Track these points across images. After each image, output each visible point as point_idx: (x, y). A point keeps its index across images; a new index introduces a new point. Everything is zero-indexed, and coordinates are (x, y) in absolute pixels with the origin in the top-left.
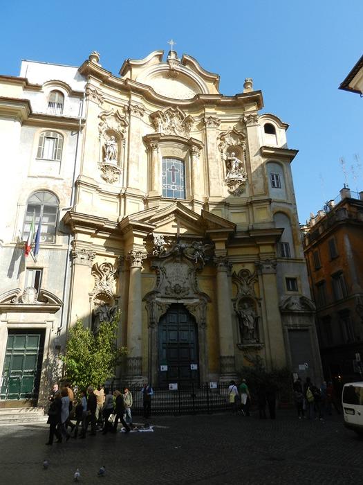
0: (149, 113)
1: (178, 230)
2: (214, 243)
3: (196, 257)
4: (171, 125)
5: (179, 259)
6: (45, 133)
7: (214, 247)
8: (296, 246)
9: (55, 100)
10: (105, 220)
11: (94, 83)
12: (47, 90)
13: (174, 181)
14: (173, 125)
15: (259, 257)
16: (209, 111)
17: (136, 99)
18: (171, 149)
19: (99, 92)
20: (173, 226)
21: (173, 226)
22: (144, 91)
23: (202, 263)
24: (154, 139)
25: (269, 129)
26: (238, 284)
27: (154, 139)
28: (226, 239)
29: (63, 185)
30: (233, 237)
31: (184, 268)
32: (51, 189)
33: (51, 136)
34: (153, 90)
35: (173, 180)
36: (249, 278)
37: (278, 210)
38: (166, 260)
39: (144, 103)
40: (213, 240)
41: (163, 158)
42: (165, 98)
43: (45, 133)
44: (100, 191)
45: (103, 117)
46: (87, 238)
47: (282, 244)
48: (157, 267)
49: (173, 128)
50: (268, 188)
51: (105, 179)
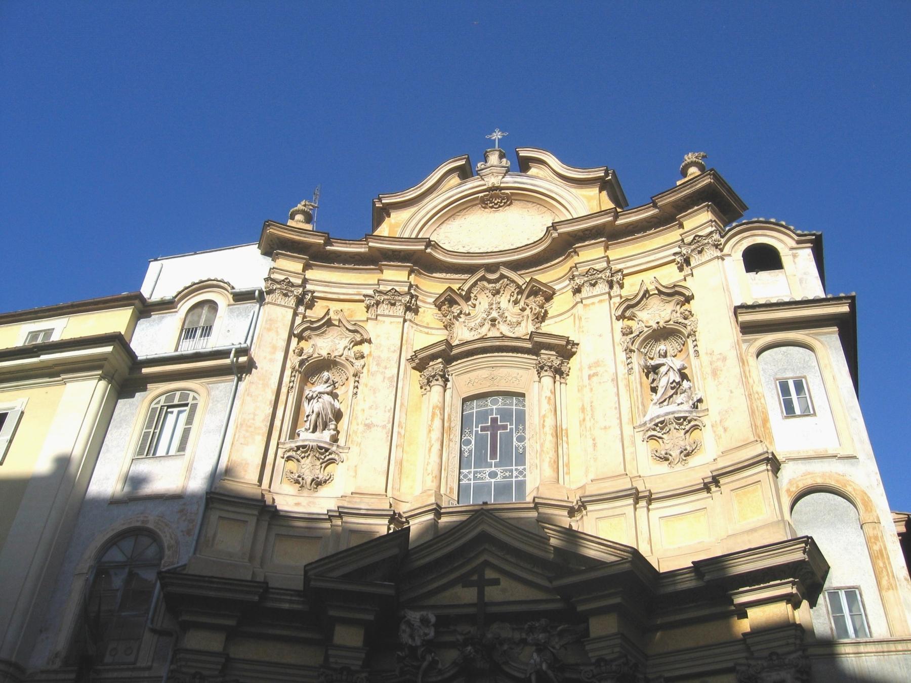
0: (432, 300)
1: (481, 594)
2: (584, 618)
6: (163, 398)
7: (587, 629)
8: (884, 593)
9: (198, 322)
10: (265, 588)
11: (291, 266)
12: (184, 307)
13: (493, 456)
14: (494, 314)
15: (748, 648)
16: (591, 254)
18: (484, 373)
22: (415, 252)
24: (434, 357)
25: (762, 259)
27: (434, 357)
28: (617, 600)
29: (182, 511)
32: (151, 526)
33: (176, 402)
34: (436, 246)
35: (493, 456)
37: (809, 482)
40: (581, 608)
41: (465, 400)
42: (469, 254)
43: (163, 398)
46: (213, 642)
47: (834, 595)
49: (493, 320)
50: (765, 421)
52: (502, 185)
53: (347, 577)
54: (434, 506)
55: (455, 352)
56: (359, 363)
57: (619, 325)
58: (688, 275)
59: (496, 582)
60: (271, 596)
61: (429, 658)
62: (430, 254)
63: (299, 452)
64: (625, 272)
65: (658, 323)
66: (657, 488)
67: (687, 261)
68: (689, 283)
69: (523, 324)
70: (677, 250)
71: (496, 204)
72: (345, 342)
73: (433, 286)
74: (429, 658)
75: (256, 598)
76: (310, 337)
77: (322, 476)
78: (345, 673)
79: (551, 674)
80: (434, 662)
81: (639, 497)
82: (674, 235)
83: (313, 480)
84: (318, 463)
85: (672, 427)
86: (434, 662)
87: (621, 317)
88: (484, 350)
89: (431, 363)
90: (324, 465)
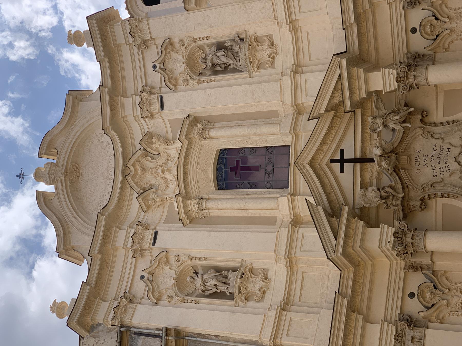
1: (349, 161)
3: (398, 127)
4: (158, 174)
5: (404, 160)
17: (122, 237)
19: (116, 303)
20: (342, 170)
21: (342, 170)
23: (410, 113)
26: (449, 40)
28: (362, 70)
30: (358, 58)
31: (422, 145)
36: (437, 19)
38: (407, 181)
39: (127, 224)
40: (364, 95)
44: (285, 306)
45: (157, 295)
48: (422, 200)
51: (264, 292)
52: (64, 167)
53: (336, 238)
54: (290, 195)
55: (183, 191)
56: (182, 258)
57: (182, 86)
58: (155, 41)
59: (342, 152)
60: (344, 291)
61: (388, 189)
62: (109, 214)
63: (243, 292)
64: (144, 84)
65: (183, 63)
66: (290, 61)
67: (145, 42)
68: (159, 42)
69: (169, 151)
70: (135, 48)
71: (77, 175)
72: (167, 269)
73: (134, 208)
74: (388, 189)
75: (346, 300)
76: (159, 292)
77: (261, 276)
78: (397, 235)
79: (400, 115)
80: (390, 187)
81: (297, 69)
82: (125, 50)
83: (263, 281)
84: (251, 280)
85: (253, 52)
86: (390, 187)
87: (175, 86)
88: (185, 174)
89: (190, 209)
90: (253, 276)
